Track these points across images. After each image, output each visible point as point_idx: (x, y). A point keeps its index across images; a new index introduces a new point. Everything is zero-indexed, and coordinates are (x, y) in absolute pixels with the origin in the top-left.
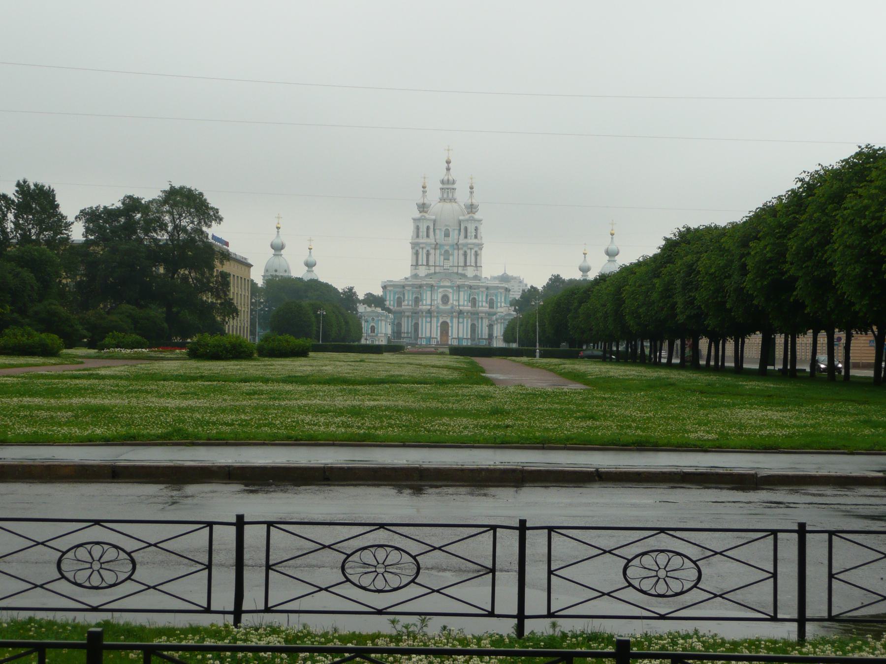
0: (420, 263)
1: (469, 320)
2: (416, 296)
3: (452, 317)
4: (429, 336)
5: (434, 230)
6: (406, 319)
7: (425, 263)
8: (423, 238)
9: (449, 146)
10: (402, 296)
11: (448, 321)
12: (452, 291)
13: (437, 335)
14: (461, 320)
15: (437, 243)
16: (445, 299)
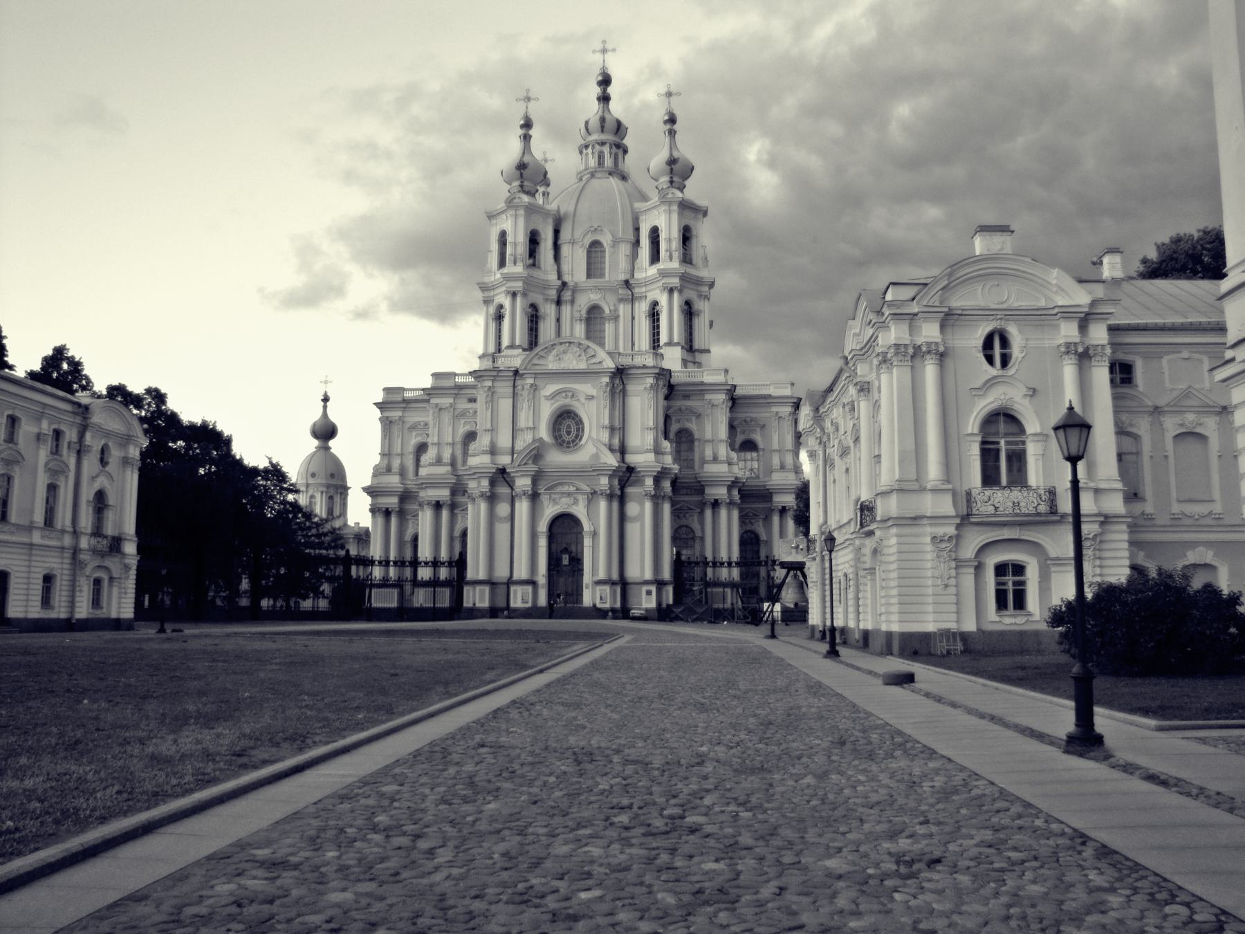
0: (506, 342)
1: (667, 508)
5: (556, 247)
8: (515, 263)
9: (604, 42)
11: (580, 511)
14: (632, 509)
15: (564, 284)
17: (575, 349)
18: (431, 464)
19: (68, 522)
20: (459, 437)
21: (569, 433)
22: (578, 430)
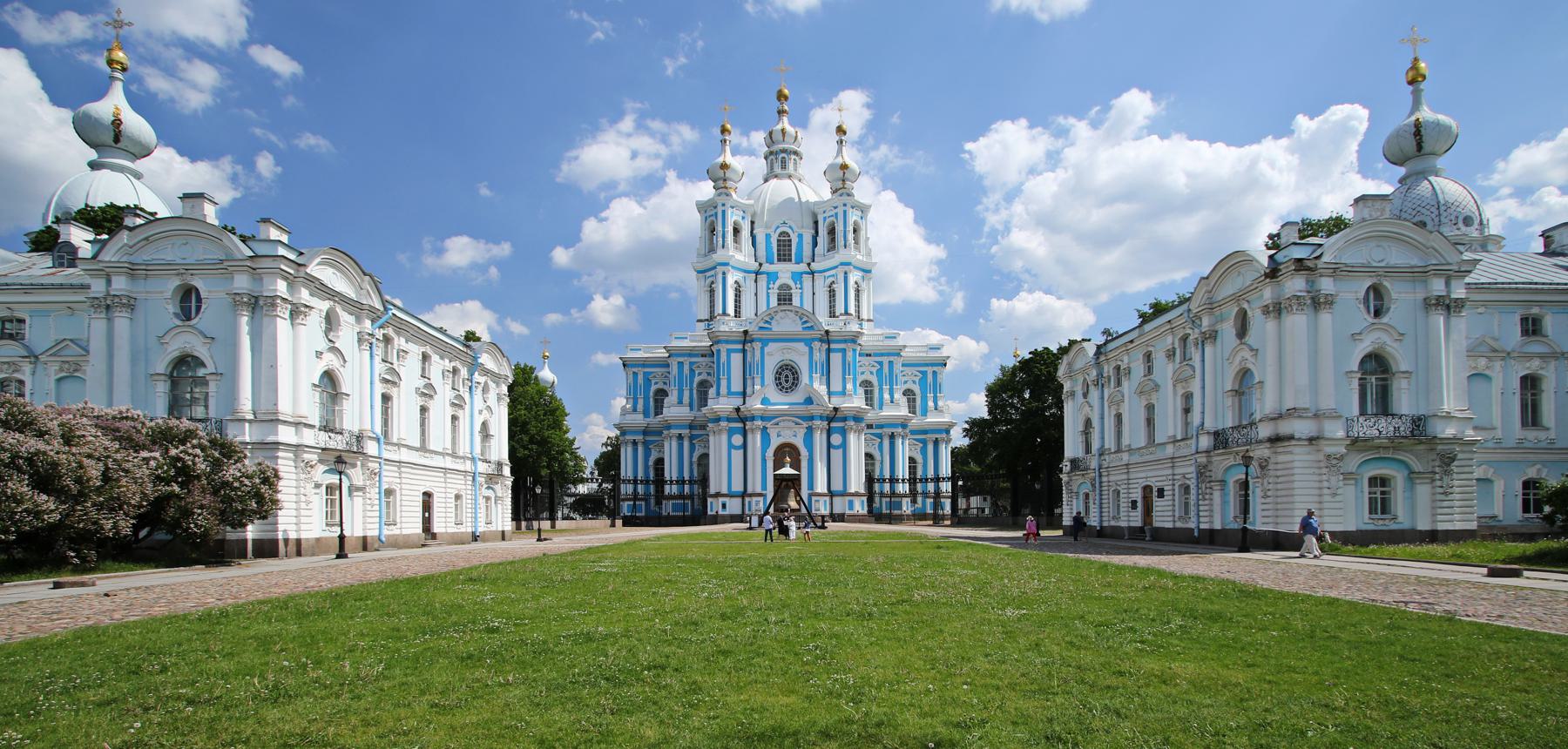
2: (701, 377)
3: (810, 430)
4: (742, 489)
6: (674, 443)
7: (731, 310)
8: (723, 247)
10: (665, 387)
11: (799, 442)
12: (806, 349)
13: (764, 487)
14: (836, 439)
16: (787, 377)
17: (792, 315)
18: (673, 405)
19: (468, 450)
20: (695, 386)
21: (787, 381)
22: (794, 379)
